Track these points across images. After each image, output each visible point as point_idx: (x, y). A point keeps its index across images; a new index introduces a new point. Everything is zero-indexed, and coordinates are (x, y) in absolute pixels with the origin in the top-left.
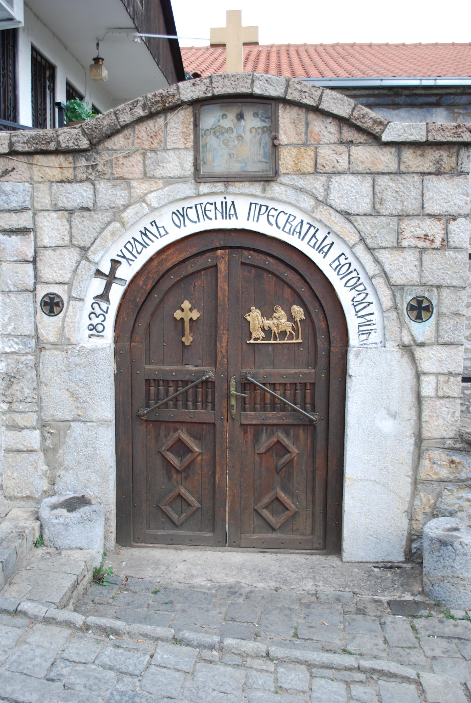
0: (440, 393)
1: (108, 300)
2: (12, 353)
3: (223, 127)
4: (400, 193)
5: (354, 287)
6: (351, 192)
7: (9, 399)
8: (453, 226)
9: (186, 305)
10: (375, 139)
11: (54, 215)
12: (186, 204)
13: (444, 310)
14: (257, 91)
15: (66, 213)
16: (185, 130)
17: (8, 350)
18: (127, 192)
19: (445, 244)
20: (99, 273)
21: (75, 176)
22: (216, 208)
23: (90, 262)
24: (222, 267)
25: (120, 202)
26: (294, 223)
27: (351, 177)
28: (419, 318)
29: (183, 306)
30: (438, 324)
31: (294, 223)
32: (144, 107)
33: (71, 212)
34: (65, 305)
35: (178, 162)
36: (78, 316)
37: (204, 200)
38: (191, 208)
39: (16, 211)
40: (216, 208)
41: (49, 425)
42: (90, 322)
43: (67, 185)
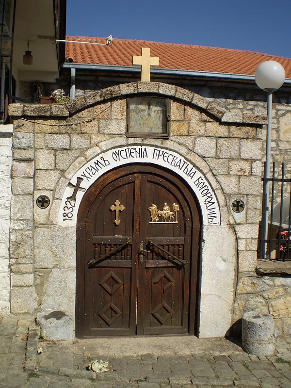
0: (248, 249)
1: (75, 200)
2: (19, 230)
3: (141, 109)
4: (229, 148)
5: (206, 194)
6: (205, 146)
7: (17, 256)
8: (254, 165)
9: (117, 202)
10: (217, 120)
11: (46, 151)
12: (120, 149)
13: (249, 207)
14: (161, 92)
15: (53, 151)
16: (121, 109)
17: (17, 228)
18: (88, 141)
19: (251, 174)
20: (70, 184)
21: (59, 130)
22: (136, 152)
23: (66, 178)
24: (137, 182)
25: (84, 146)
26: (177, 161)
27: (206, 138)
28: (238, 210)
29: (115, 203)
30: (247, 214)
31: (177, 161)
32: (101, 96)
33: (56, 150)
34: (51, 202)
35: (117, 126)
36: (58, 209)
37: (130, 147)
38: (123, 151)
39: (24, 149)
40: (136, 152)
41: (39, 271)
42: (64, 212)
43: (55, 136)
